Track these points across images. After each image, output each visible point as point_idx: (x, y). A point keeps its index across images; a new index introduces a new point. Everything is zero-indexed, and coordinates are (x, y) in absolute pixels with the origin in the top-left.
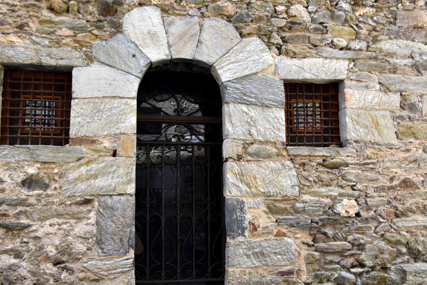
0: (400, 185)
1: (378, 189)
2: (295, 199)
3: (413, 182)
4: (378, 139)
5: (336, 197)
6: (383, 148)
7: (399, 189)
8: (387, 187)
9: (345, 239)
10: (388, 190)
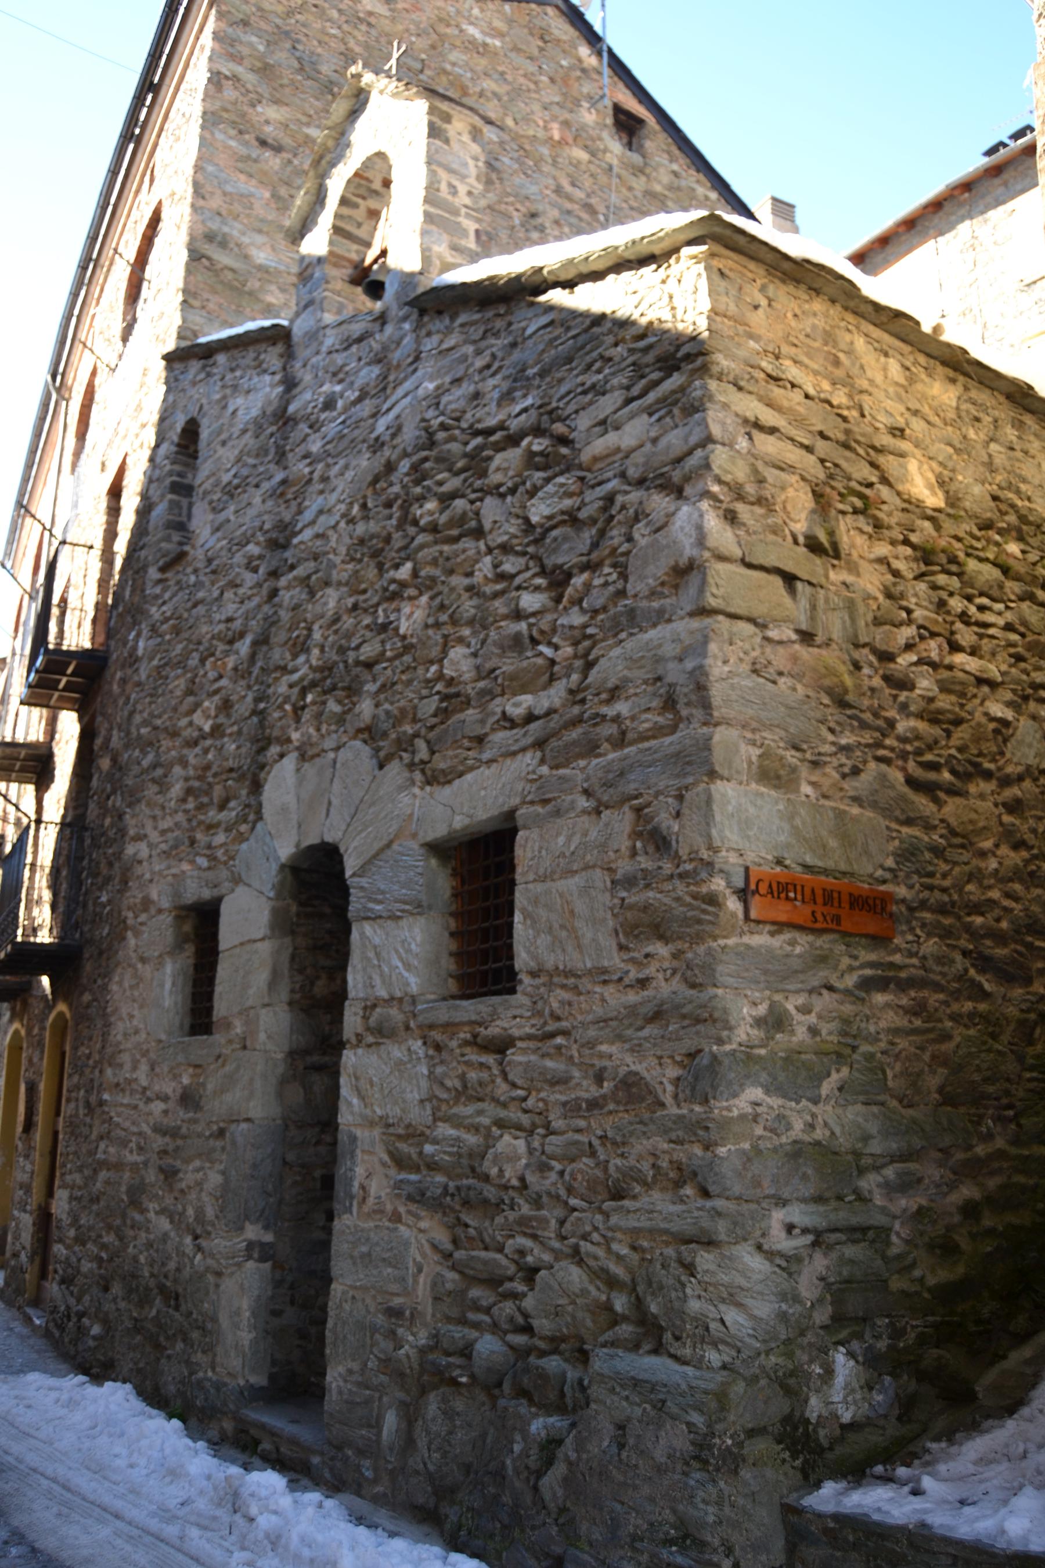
0: (613, 1096)
1: (571, 1109)
2: (422, 1134)
3: (647, 1084)
4: (575, 960)
5: (488, 1129)
6: (585, 984)
7: (611, 1106)
8: (587, 1101)
9: (500, 1250)
10: (588, 1110)
